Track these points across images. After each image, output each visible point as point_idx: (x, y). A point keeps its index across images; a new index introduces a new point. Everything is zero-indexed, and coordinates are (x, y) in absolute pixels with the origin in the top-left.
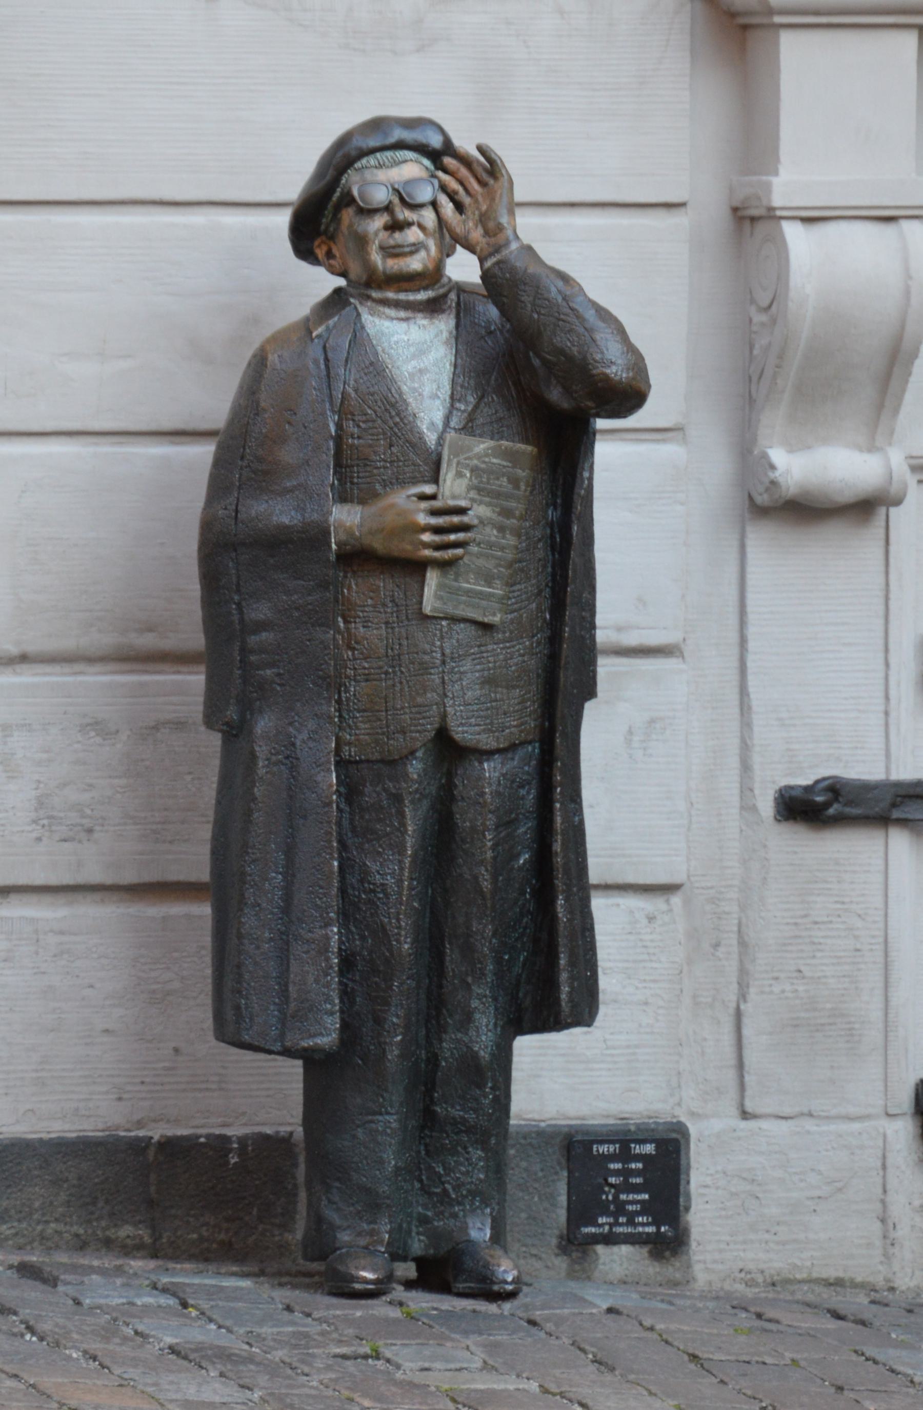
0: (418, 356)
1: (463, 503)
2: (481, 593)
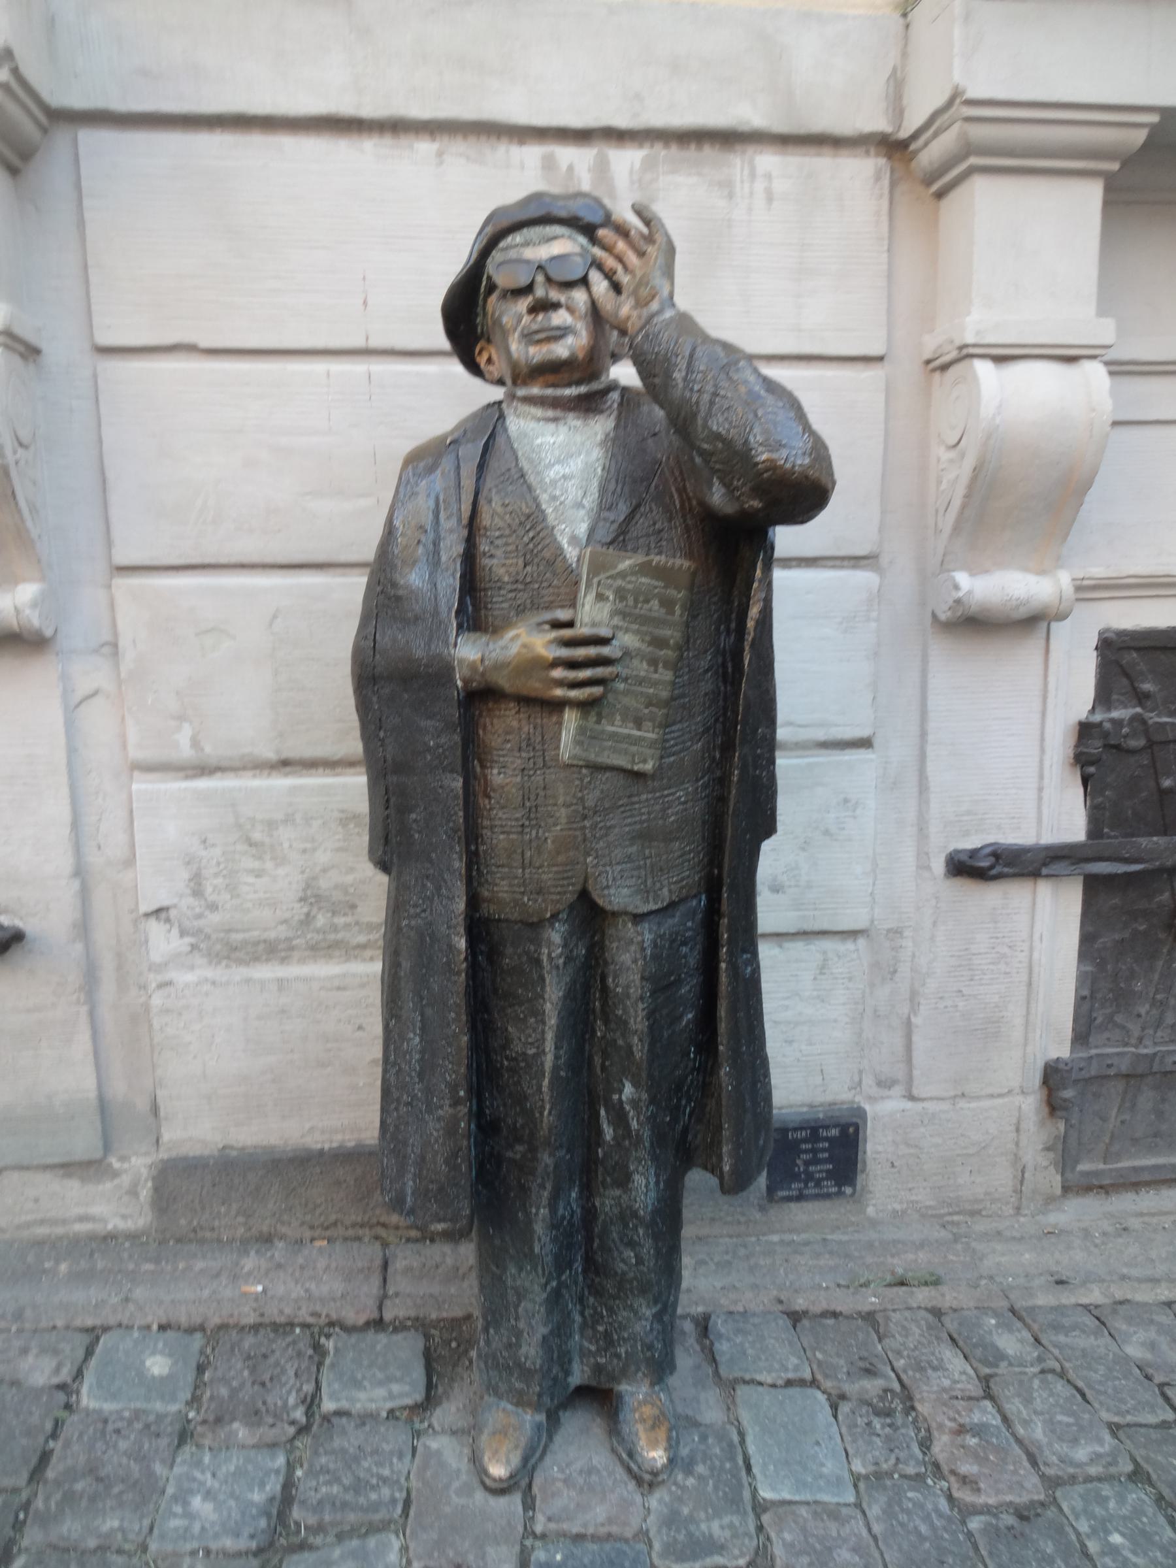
0: (565, 462)
1: (604, 632)
2: (629, 736)
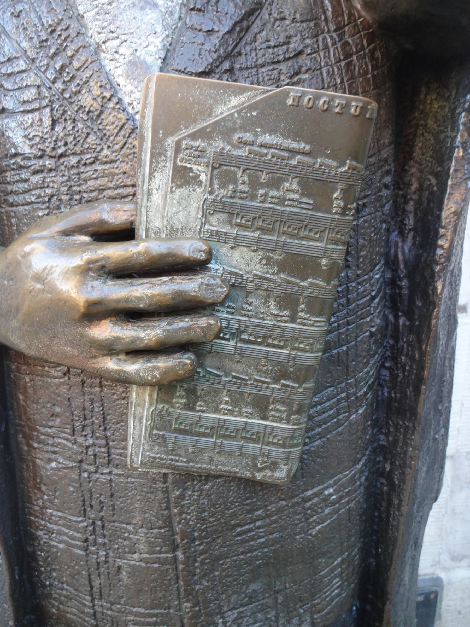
1: (189, 248)
